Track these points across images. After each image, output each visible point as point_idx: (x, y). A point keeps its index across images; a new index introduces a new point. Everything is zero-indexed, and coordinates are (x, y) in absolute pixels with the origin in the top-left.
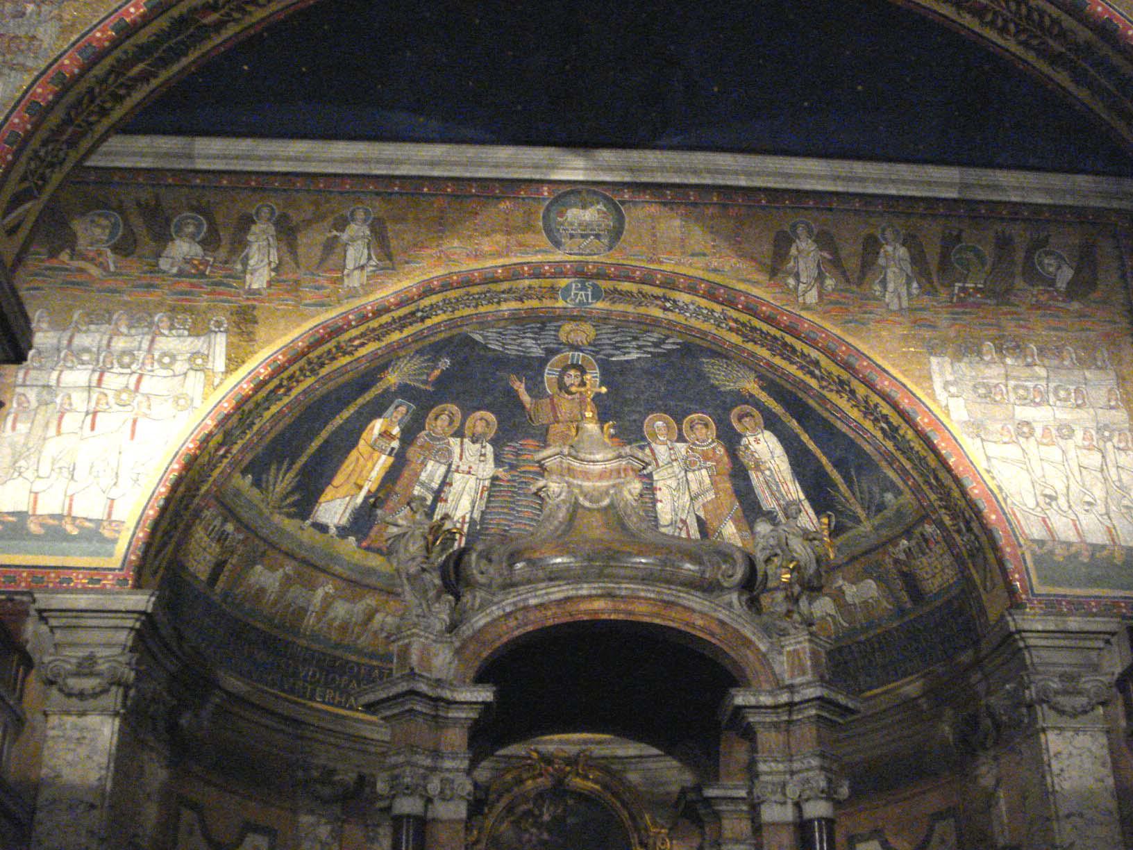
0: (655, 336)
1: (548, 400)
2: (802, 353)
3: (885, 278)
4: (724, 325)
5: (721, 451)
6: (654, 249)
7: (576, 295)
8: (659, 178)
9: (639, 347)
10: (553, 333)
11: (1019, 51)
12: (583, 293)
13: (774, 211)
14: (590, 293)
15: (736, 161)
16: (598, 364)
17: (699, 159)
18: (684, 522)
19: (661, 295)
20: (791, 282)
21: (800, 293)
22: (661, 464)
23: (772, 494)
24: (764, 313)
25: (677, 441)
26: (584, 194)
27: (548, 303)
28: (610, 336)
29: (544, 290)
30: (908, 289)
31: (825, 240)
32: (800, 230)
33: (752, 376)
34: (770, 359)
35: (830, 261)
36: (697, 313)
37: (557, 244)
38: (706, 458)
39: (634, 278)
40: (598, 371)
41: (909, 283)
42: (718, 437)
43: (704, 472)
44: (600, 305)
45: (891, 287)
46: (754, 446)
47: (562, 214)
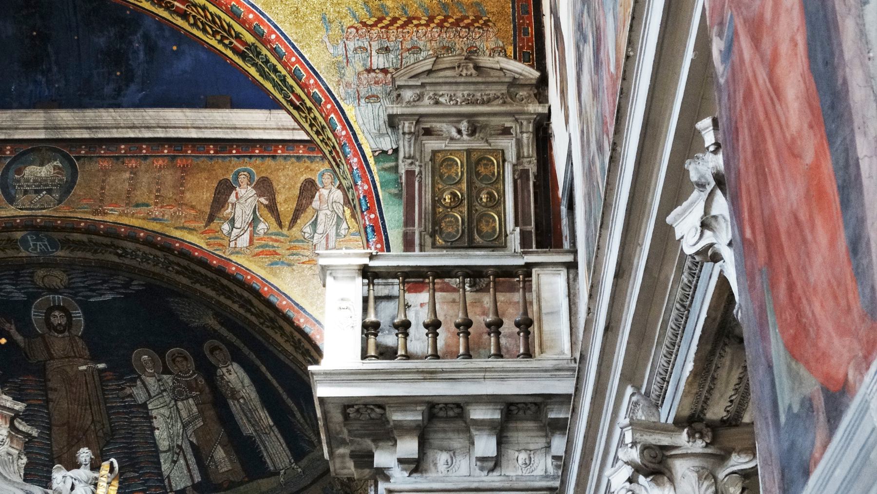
0: (120, 280)
1: (40, 339)
2: (236, 292)
3: (316, 219)
4: (170, 269)
5: (202, 382)
6: (101, 201)
7: (35, 245)
8: (116, 134)
9: (112, 289)
10: (28, 279)
11: (220, 47)
12: (40, 243)
13: (220, 161)
14: (46, 243)
15: (186, 116)
16: (80, 306)
17: (151, 115)
18: (180, 447)
19: (109, 243)
20: (226, 227)
21: (233, 237)
22: (153, 395)
23: (249, 421)
24: (196, 257)
25: (163, 373)
26: (44, 149)
27: (10, 253)
28: (80, 280)
29: (4, 242)
30: (337, 229)
31: (265, 187)
32: (243, 179)
33: (210, 313)
34: (217, 297)
35: (266, 206)
36: (145, 258)
37: (11, 200)
38: (191, 389)
39: (80, 229)
40: (80, 311)
41: (338, 225)
42: (196, 367)
43: (191, 401)
44: (60, 253)
45: (320, 229)
46: (228, 377)
47: (19, 171)
